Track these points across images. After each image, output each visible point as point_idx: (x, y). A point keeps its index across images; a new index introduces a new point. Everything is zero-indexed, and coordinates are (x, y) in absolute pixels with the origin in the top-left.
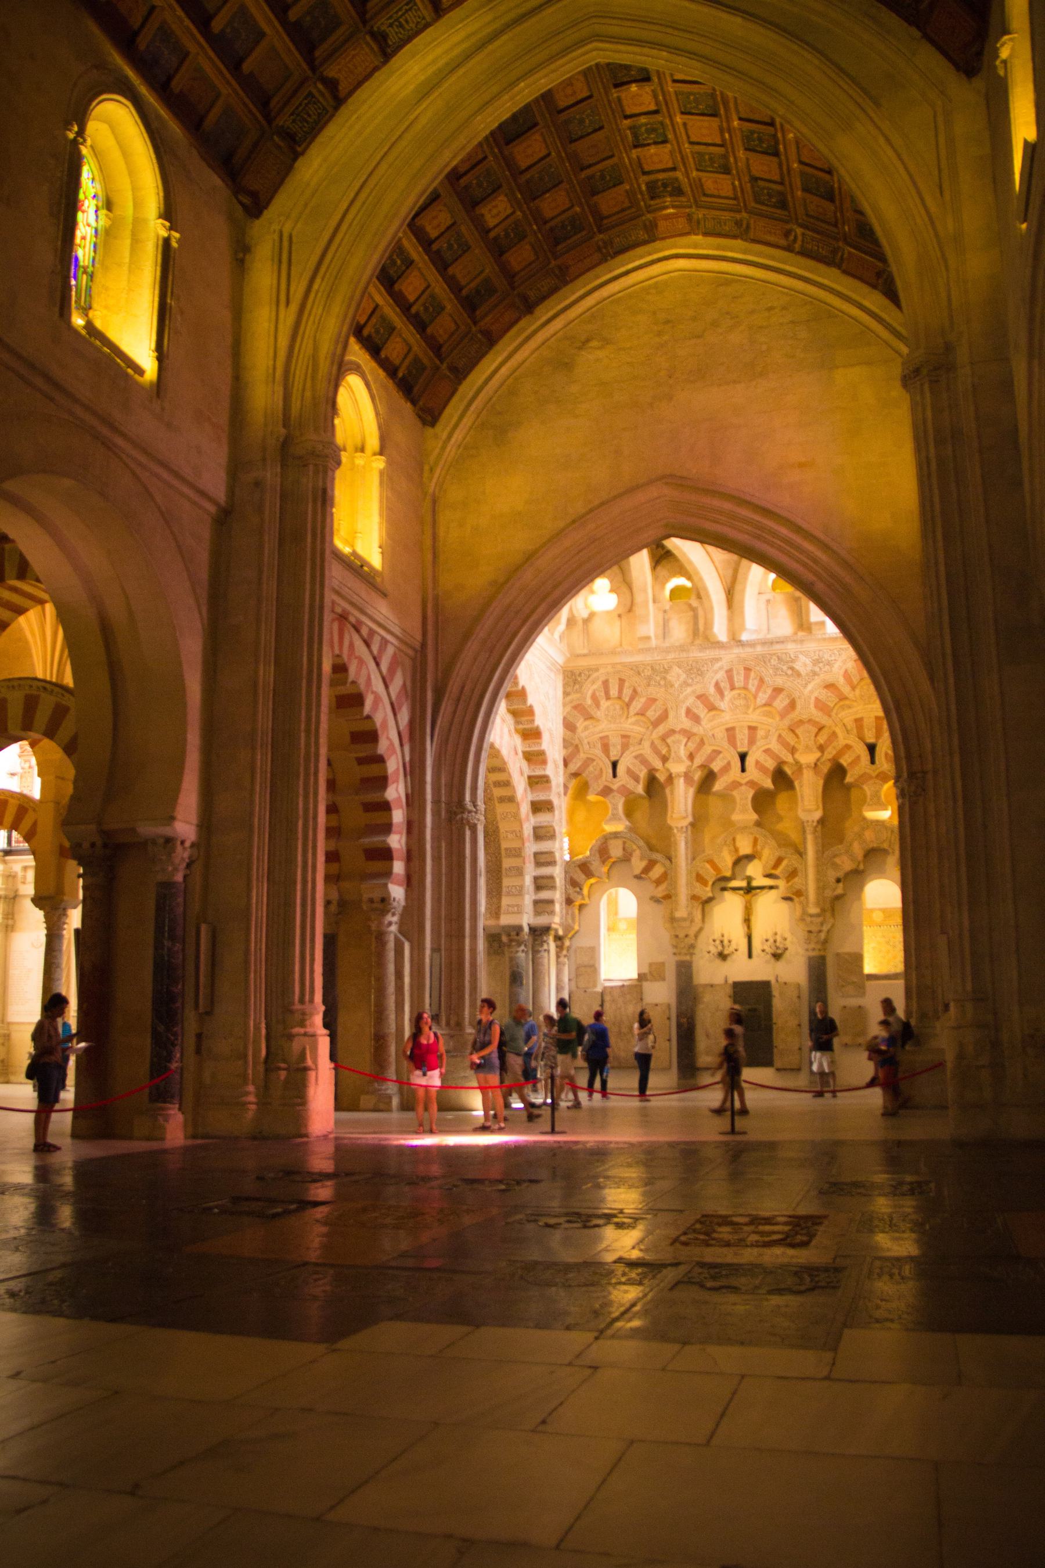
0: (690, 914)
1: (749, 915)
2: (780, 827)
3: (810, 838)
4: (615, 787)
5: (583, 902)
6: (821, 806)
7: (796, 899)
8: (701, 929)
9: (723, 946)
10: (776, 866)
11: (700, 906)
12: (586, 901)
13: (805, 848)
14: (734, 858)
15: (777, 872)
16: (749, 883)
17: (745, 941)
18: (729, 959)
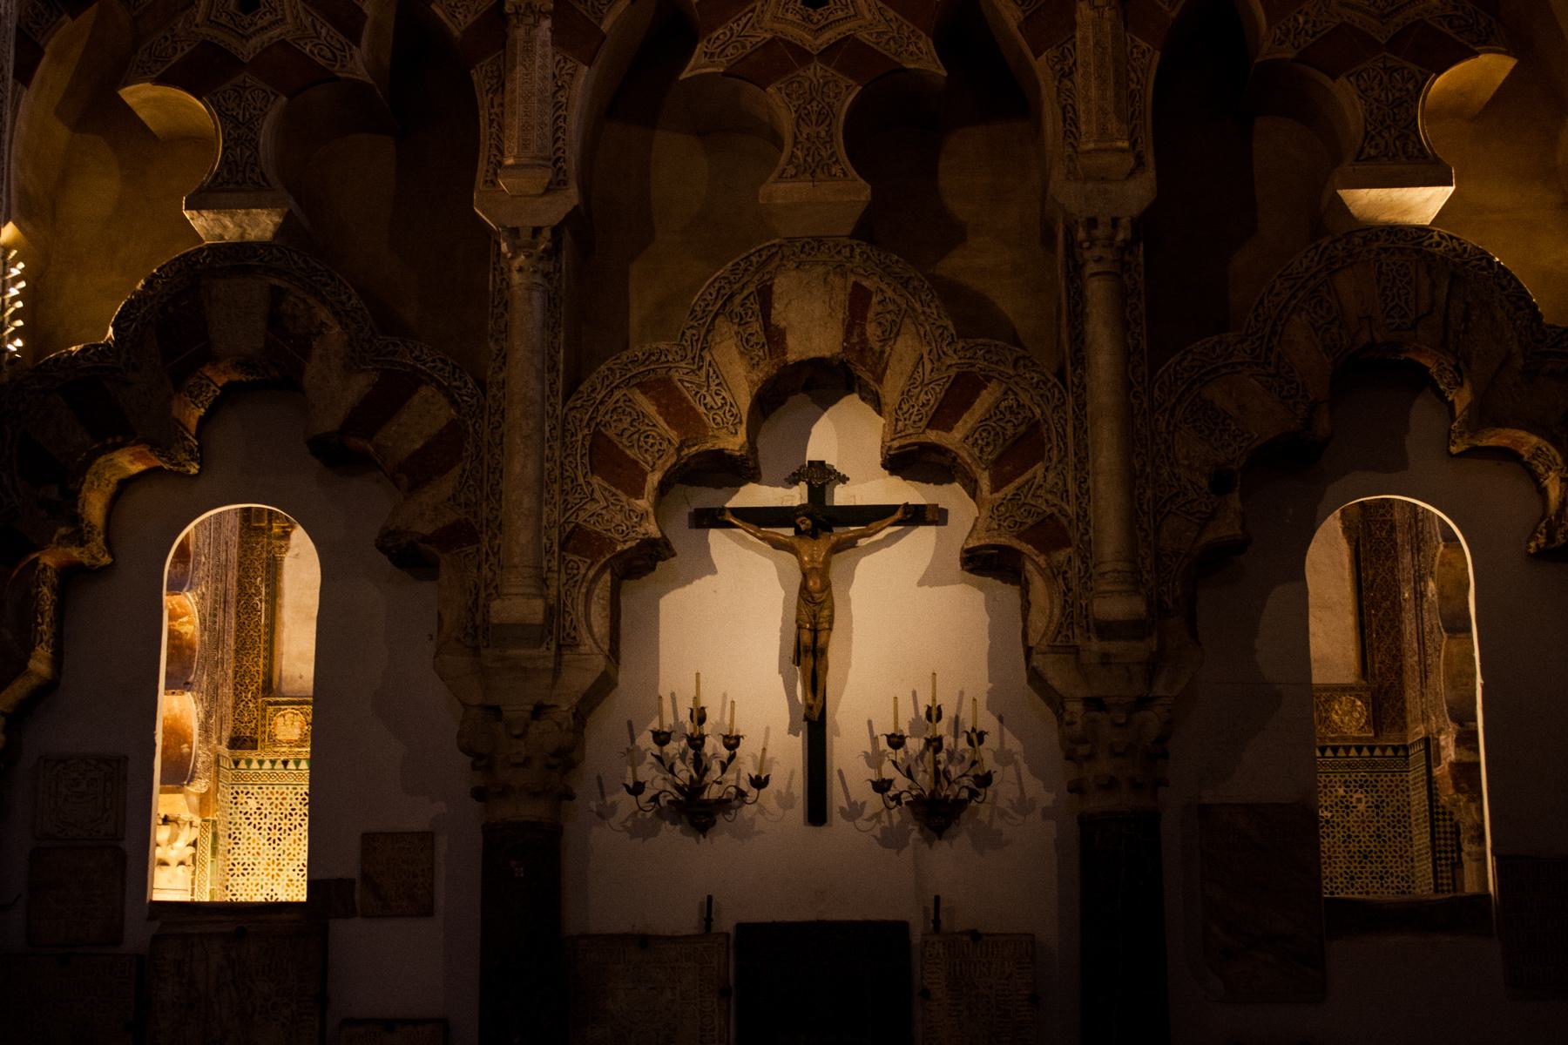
0: (554, 613)
1: (815, 631)
2: (955, 265)
3: (1097, 292)
4: (248, 50)
5: (75, 553)
6: (1150, 159)
7: (1034, 563)
8: (605, 684)
9: (700, 765)
10: (943, 417)
11: (607, 577)
12: (94, 553)
13: (1079, 339)
14: (766, 369)
15: (953, 439)
16: (818, 494)
17: (788, 753)
18: (720, 819)
